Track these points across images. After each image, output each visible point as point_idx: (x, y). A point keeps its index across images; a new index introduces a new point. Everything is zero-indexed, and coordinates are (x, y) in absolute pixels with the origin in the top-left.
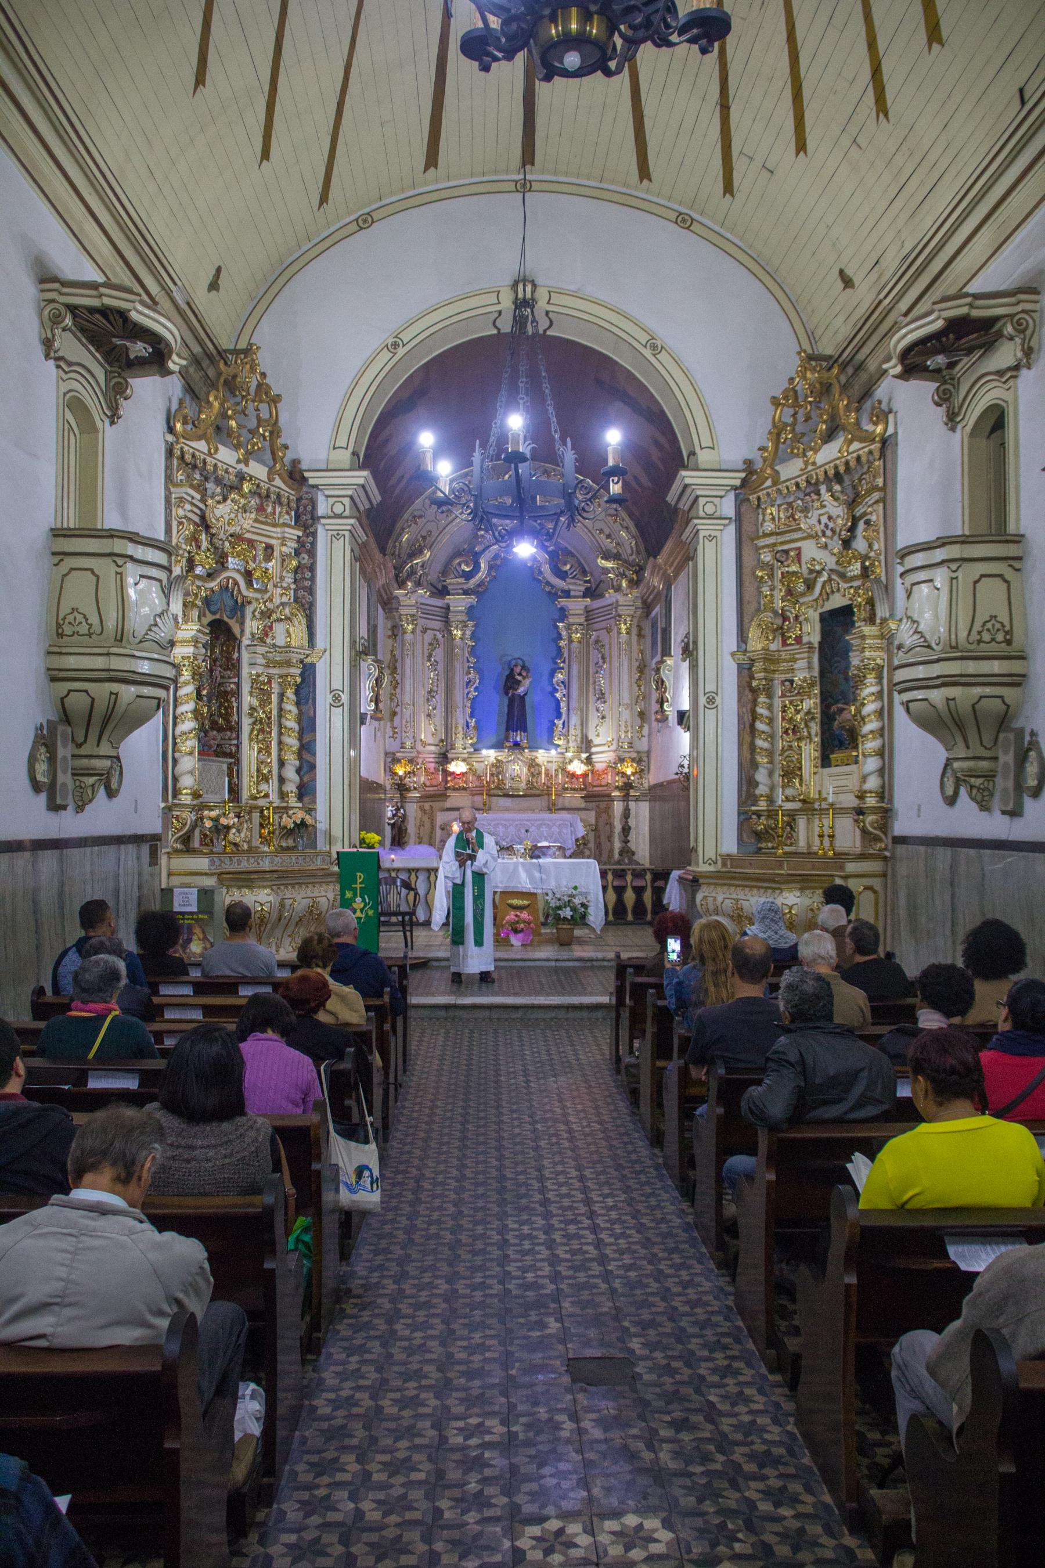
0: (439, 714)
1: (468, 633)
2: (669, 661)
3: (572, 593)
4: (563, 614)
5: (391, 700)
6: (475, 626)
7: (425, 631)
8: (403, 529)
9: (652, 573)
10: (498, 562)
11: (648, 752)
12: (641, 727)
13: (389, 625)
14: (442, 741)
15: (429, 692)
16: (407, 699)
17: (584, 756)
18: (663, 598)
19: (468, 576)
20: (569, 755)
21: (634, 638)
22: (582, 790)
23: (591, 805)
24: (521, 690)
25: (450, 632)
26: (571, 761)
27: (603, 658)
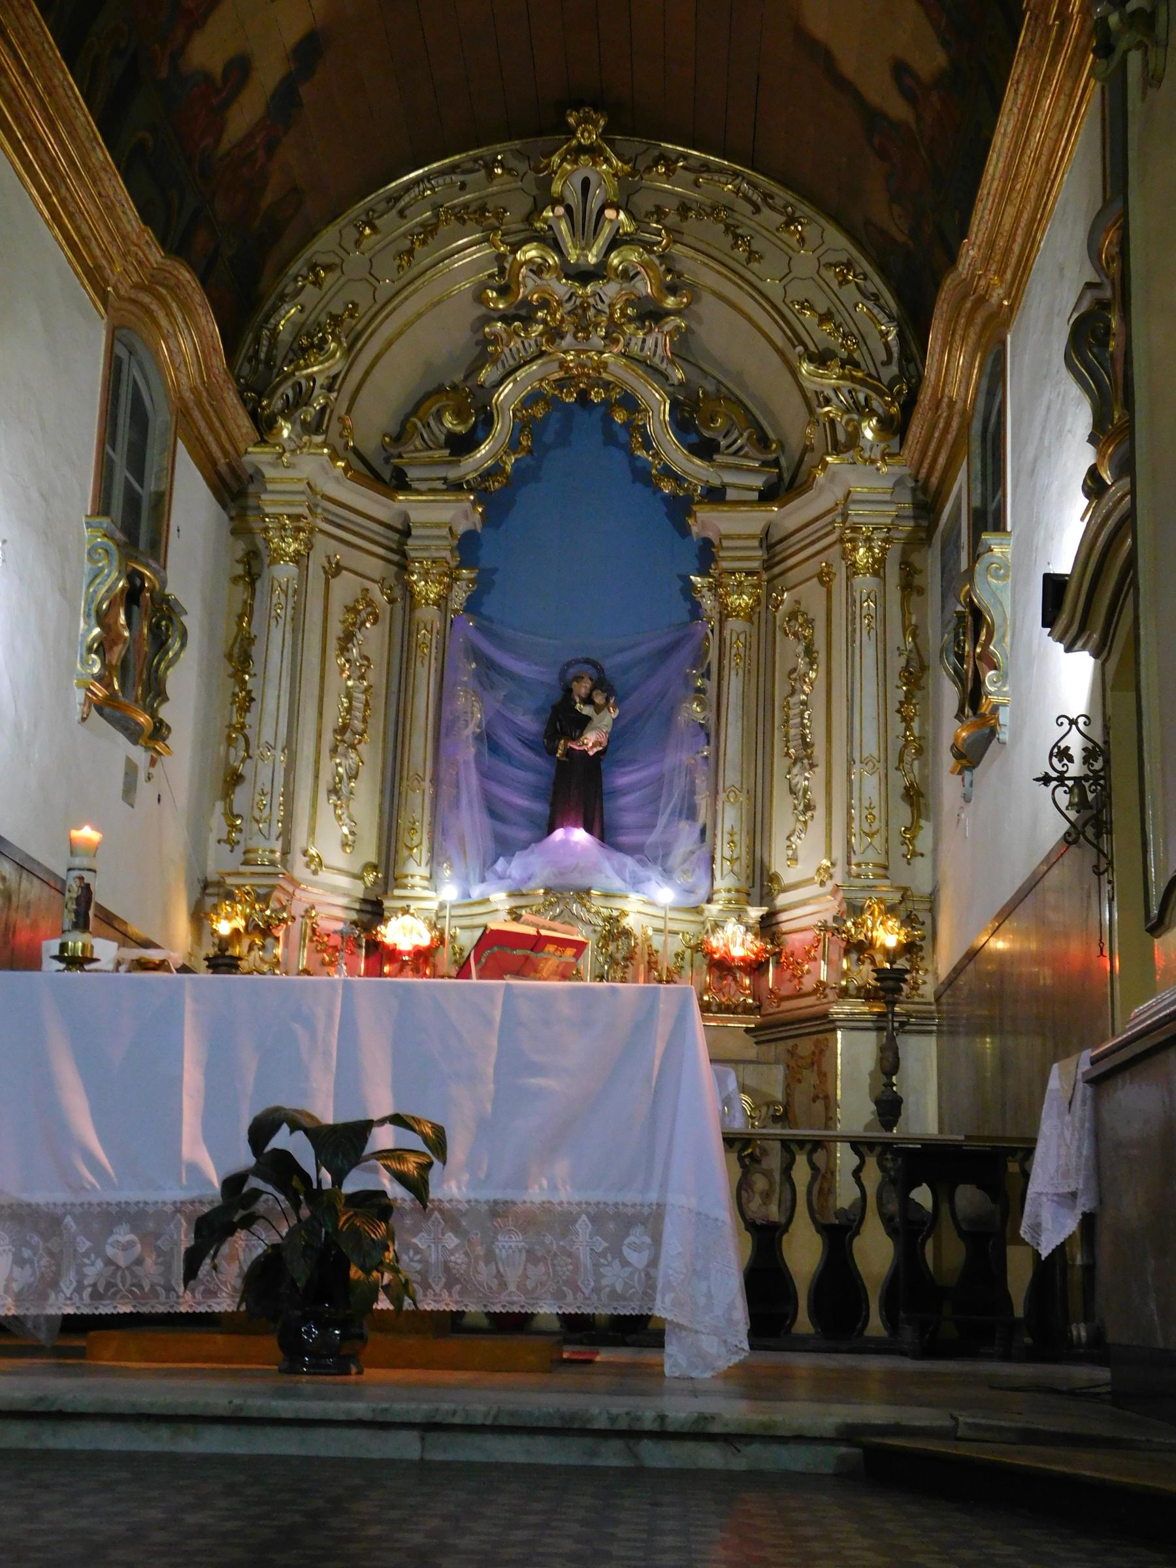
0: (365, 798)
1: (460, 595)
2: (999, 548)
3: (731, 495)
4: (706, 554)
5: (230, 741)
6: (483, 586)
7: (335, 570)
8: (282, 298)
9: (947, 344)
10: (539, 411)
11: (932, 901)
12: (913, 828)
13: (240, 548)
14: (375, 868)
15: (343, 729)
16: (267, 735)
17: (755, 913)
18: (977, 425)
19: (462, 445)
20: (713, 909)
21: (894, 595)
22: (748, 1010)
23: (772, 1050)
24: (591, 741)
25: (408, 588)
26: (717, 926)
27: (809, 652)
